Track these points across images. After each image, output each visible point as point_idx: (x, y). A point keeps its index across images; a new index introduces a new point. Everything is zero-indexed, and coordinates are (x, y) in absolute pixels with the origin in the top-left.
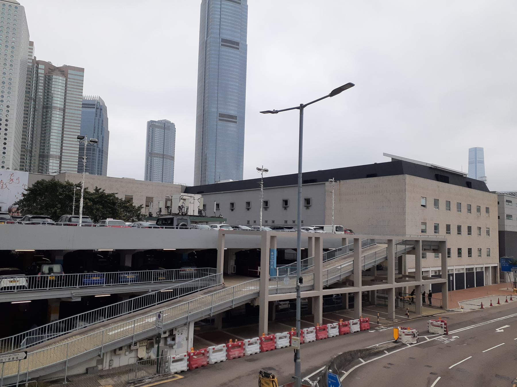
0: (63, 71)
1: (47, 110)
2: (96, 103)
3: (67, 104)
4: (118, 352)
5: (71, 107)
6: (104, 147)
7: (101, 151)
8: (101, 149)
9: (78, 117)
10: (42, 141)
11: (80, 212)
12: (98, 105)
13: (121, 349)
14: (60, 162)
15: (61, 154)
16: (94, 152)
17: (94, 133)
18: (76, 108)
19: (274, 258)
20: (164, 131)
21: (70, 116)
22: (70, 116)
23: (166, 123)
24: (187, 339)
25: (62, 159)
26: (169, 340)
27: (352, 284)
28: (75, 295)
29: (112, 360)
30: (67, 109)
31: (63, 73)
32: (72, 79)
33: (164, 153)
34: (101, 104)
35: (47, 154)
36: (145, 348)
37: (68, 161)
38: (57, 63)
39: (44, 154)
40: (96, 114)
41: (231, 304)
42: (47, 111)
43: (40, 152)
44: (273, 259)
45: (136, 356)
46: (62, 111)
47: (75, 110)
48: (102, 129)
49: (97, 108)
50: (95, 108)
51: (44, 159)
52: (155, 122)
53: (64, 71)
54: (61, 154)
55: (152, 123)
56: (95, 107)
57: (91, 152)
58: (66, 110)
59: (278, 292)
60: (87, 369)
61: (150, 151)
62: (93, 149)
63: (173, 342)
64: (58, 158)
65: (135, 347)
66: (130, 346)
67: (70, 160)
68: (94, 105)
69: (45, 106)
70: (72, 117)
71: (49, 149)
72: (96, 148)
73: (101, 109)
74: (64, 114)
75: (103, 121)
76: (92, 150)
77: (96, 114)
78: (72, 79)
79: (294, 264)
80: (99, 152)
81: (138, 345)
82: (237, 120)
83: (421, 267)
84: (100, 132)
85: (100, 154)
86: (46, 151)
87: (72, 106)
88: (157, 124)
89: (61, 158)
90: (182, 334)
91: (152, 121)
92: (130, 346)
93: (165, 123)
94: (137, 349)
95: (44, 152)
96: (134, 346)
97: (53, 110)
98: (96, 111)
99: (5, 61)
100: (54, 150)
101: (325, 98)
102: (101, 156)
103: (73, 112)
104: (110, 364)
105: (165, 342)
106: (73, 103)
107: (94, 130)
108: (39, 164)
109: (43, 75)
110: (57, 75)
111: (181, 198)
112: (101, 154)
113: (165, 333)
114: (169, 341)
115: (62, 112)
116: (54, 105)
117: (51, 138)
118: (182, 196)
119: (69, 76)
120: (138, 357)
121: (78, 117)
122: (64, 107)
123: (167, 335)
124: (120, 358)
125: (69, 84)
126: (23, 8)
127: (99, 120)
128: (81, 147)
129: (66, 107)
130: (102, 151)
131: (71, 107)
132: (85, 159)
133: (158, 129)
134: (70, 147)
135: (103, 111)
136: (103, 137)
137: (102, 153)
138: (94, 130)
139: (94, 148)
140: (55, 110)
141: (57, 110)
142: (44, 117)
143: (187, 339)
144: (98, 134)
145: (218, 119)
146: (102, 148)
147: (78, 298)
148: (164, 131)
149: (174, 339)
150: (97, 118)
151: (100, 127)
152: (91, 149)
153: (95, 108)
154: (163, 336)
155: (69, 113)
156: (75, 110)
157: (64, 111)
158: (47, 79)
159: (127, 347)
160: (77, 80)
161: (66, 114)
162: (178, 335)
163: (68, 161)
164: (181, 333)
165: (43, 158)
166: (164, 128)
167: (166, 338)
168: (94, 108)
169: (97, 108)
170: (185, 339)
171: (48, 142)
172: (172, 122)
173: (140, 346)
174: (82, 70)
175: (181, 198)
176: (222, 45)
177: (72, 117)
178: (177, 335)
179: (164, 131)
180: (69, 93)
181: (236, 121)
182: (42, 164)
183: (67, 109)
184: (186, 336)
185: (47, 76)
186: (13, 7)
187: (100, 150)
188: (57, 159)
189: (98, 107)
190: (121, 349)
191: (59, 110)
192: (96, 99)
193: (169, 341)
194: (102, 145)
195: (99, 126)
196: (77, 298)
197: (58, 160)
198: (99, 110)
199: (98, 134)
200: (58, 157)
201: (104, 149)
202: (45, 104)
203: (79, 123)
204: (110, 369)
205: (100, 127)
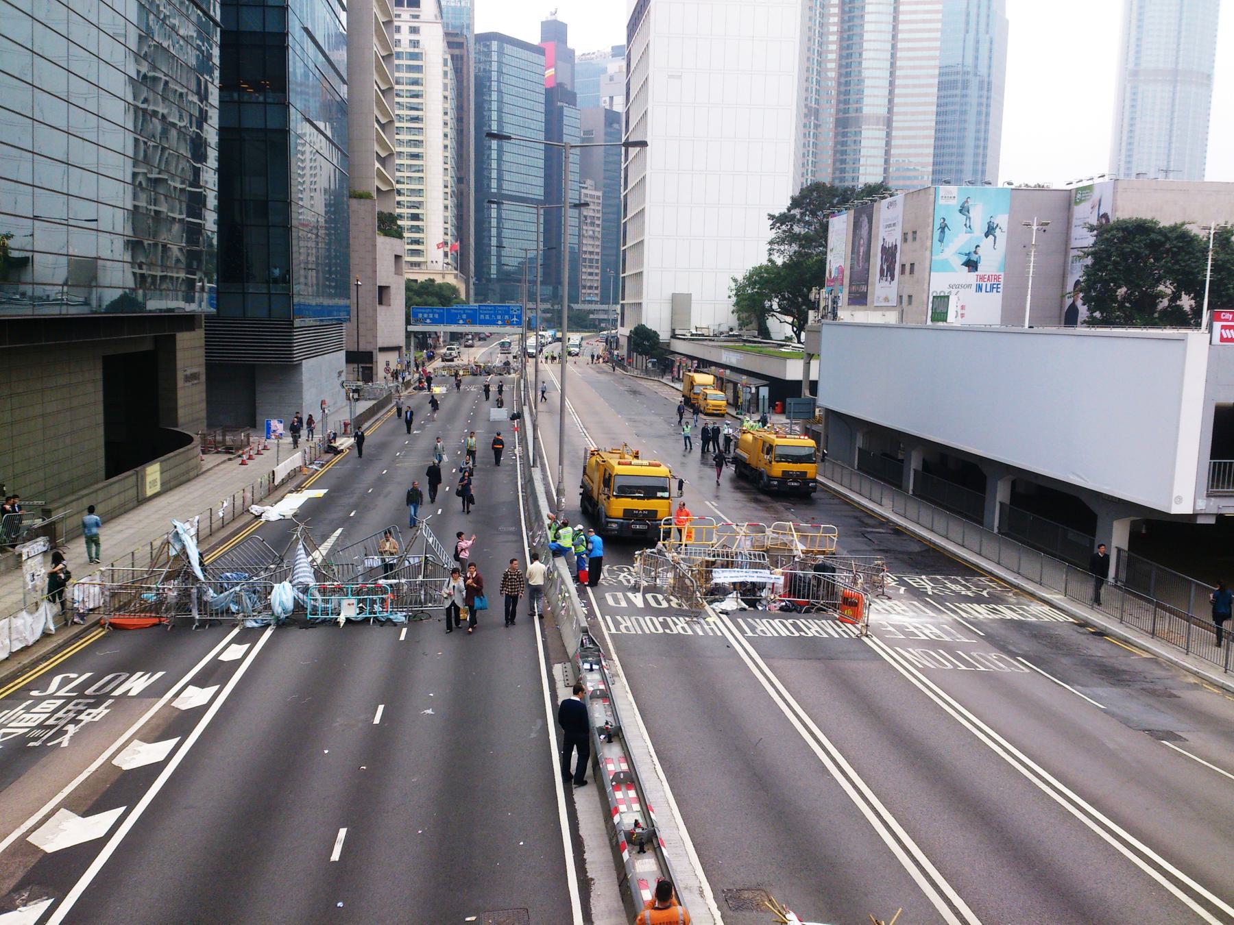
6: (994, 70)
7: (986, 86)
8: (986, 80)
10: (843, 80)
14: (888, 135)
15: (890, 111)
16: (965, 92)
17: (967, 32)
25: (894, 124)
33: (1177, 63)
35: (854, 115)
37: (909, 128)
39: (847, 115)
43: (838, 111)
48: (988, 16)
51: (849, 130)
54: (890, 111)
57: (958, 92)
62: (963, 81)
64: (882, 123)
67: (913, 124)
71: (859, 101)
72: (971, 77)
76: (960, 85)
80: (981, 88)
84: (982, 27)
85: (981, 97)
86: (852, 106)
89: (889, 123)
95: (846, 111)
100: (873, 102)
102: (984, 100)
107: (967, 23)
108: (835, 146)
112: (985, 93)
117: (865, 69)
128: (944, 78)
130: (989, 83)
134: (915, 86)
136: (991, 43)
137: (989, 90)
138: (967, 23)
139: (966, 77)
142: (847, 9)
144: (977, 31)
146: (989, 76)
151: (983, 12)
163: (909, 128)
165: (844, 128)
171: (856, 81)
182: (842, 146)
187: (981, 83)
188: (881, 127)
194: (990, 67)
195: (979, 7)
197: (883, 130)
199: (977, 31)
200: (881, 119)
201: (994, 79)
203: (937, 12)
205: (983, 12)
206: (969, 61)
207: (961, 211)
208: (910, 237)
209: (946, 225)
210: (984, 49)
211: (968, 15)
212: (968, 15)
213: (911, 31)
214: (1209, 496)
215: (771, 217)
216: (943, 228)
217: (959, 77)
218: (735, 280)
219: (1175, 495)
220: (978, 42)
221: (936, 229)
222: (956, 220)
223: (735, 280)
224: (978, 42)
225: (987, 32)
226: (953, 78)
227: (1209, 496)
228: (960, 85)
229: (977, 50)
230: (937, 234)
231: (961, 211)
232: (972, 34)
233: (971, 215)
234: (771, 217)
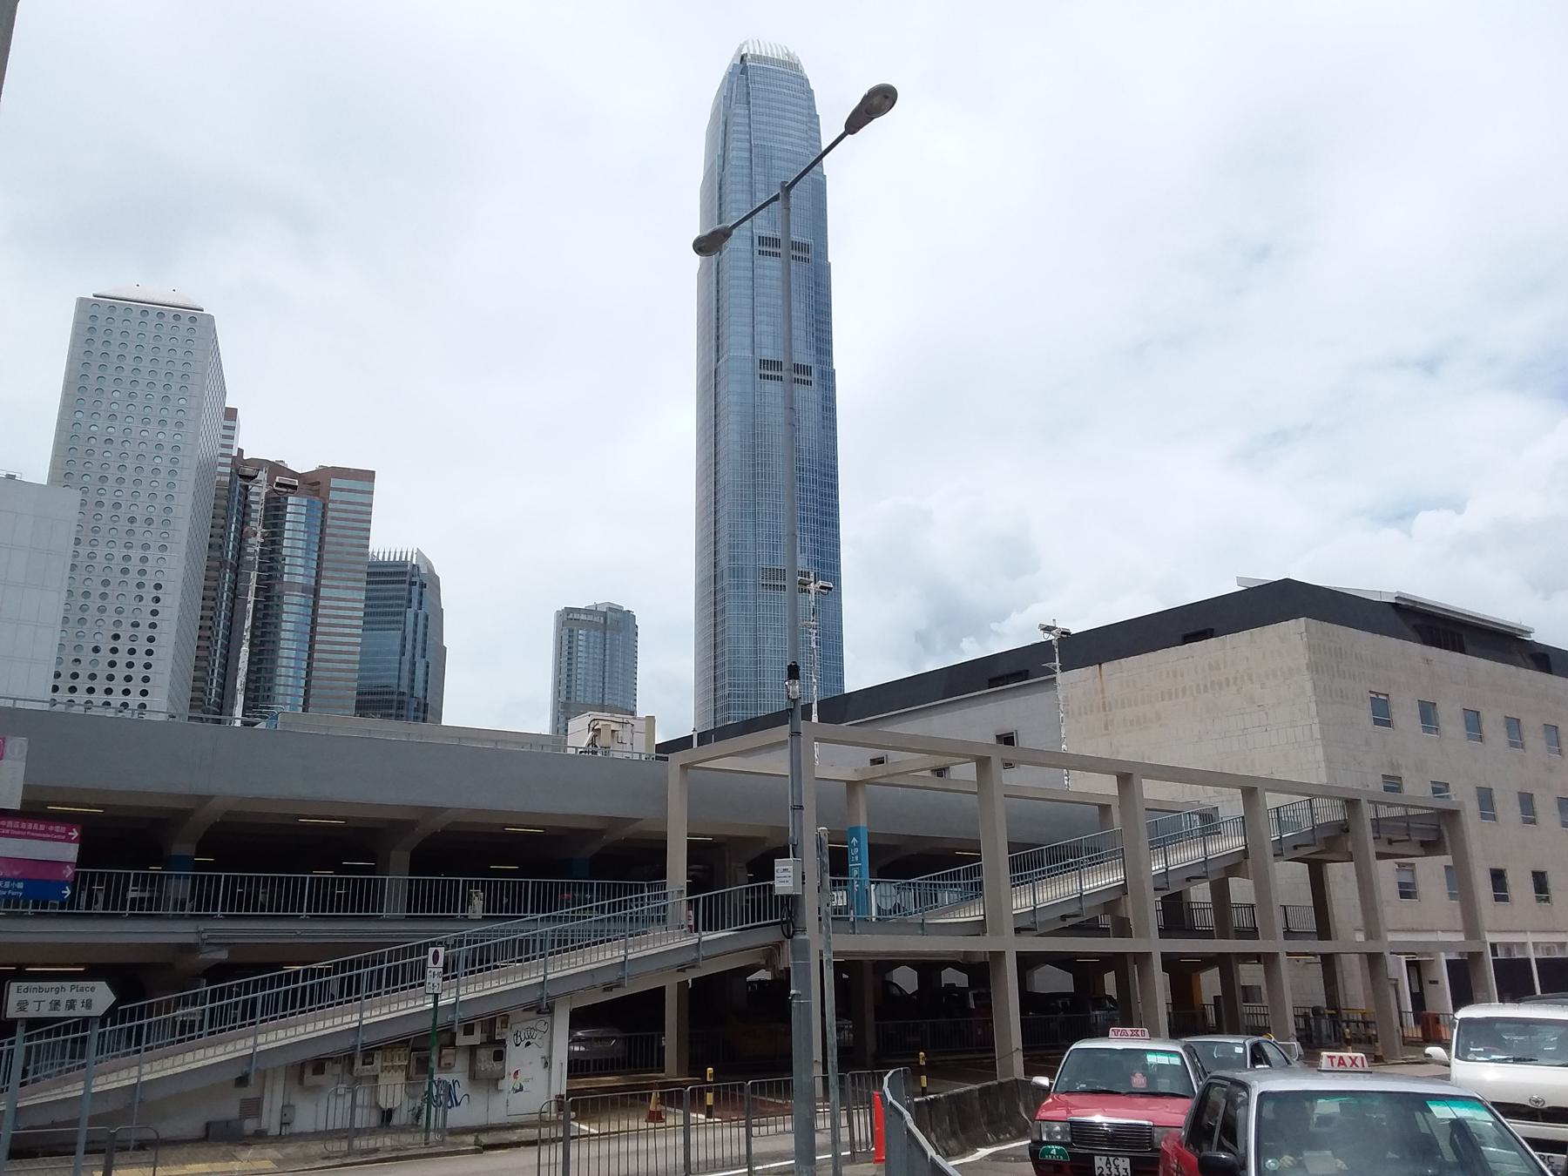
0: (316, 484)
4: (310, 1078)
7: (422, 708)
11: (238, 686)
13: (319, 1066)
19: (859, 854)
21: (332, 608)
24: (546, 1063)
26: (484, 1055)
27: (1122, 928)
28: (209, 937)
29: (292, 1106)
30: (326, 586)
31: (315, 487)
32: (342, 502)
34: (424, 571)
36: (400, 1077)
38: (302, 463)
41: (695, 955)
44: (857, 858)
45: (373, 1104)
52: (578, 610)
53: (319, 483)
55: (568, 615)
56: (407, 578)
58: (323, 592)
59: (856, 931)
60: (208, 1125)
61: (563, 699)
63: (497, 1066)
65: (369, 1067)
66: (350, 1059)
68: (405, 573)
72: (406, 698)
73: (423, 586)
74: (315, 604)
75: (427, 618)
78: (342, 502)
79: (926, 879)
81: (378, 1063)
83: (1382, 928)
90: (528, 1044)
91: (569, 611)
92: (348, 1059)
94: (377, 1076)
96: (364, 1064)
99: (89, 345)
101: (837, 144)
104: (284, 1118)
105: (470, 1060)
111: (592, 726)
113: (469, 1030)
114: (485, 1063)
118: (596, 722)
119: (333, 495)
120: (377, 1104)
123: (476, 1038)
124: (317, 1105)
125: (333, 518)
126: (211, 319)
127: (416, 616)
130: (426, 705)
132: (259, 535)
136: (428, 667)
137: (425, 712)
139: (401, 698)
140: (291, 593)
143: (547, 1064)
146: (426, 698)
147: (219, 950)
149: (499, 1056)
152: (392, 701)
154: (462, 1040)
157: (316, 593)
159: (343, 1071)
160: (358, 504)
162: (517, 1045)
164: (526, 1041)
167: (472, 1050)
168: (404, 582)
169: (413, 584)
170: (539, 1063)
172: (625, 609)
173: (384, 1069)
174: (369, 476)
175: (592, 726)
176: (761, 378)
178: (510, 1046)
184: (546, 1054)
186: (185, 320)
189: (414, 579)
190: (319, 1066)
192: (409, 559)
193: (485, 1063)
196: (215, 948)
198: (416, 589)
204: (283, 1134)
206: (405, 682)
211: (404, 639)
225: (424, 657)
226: (390, 697)
228: (395, 704)
229: (413, 673)
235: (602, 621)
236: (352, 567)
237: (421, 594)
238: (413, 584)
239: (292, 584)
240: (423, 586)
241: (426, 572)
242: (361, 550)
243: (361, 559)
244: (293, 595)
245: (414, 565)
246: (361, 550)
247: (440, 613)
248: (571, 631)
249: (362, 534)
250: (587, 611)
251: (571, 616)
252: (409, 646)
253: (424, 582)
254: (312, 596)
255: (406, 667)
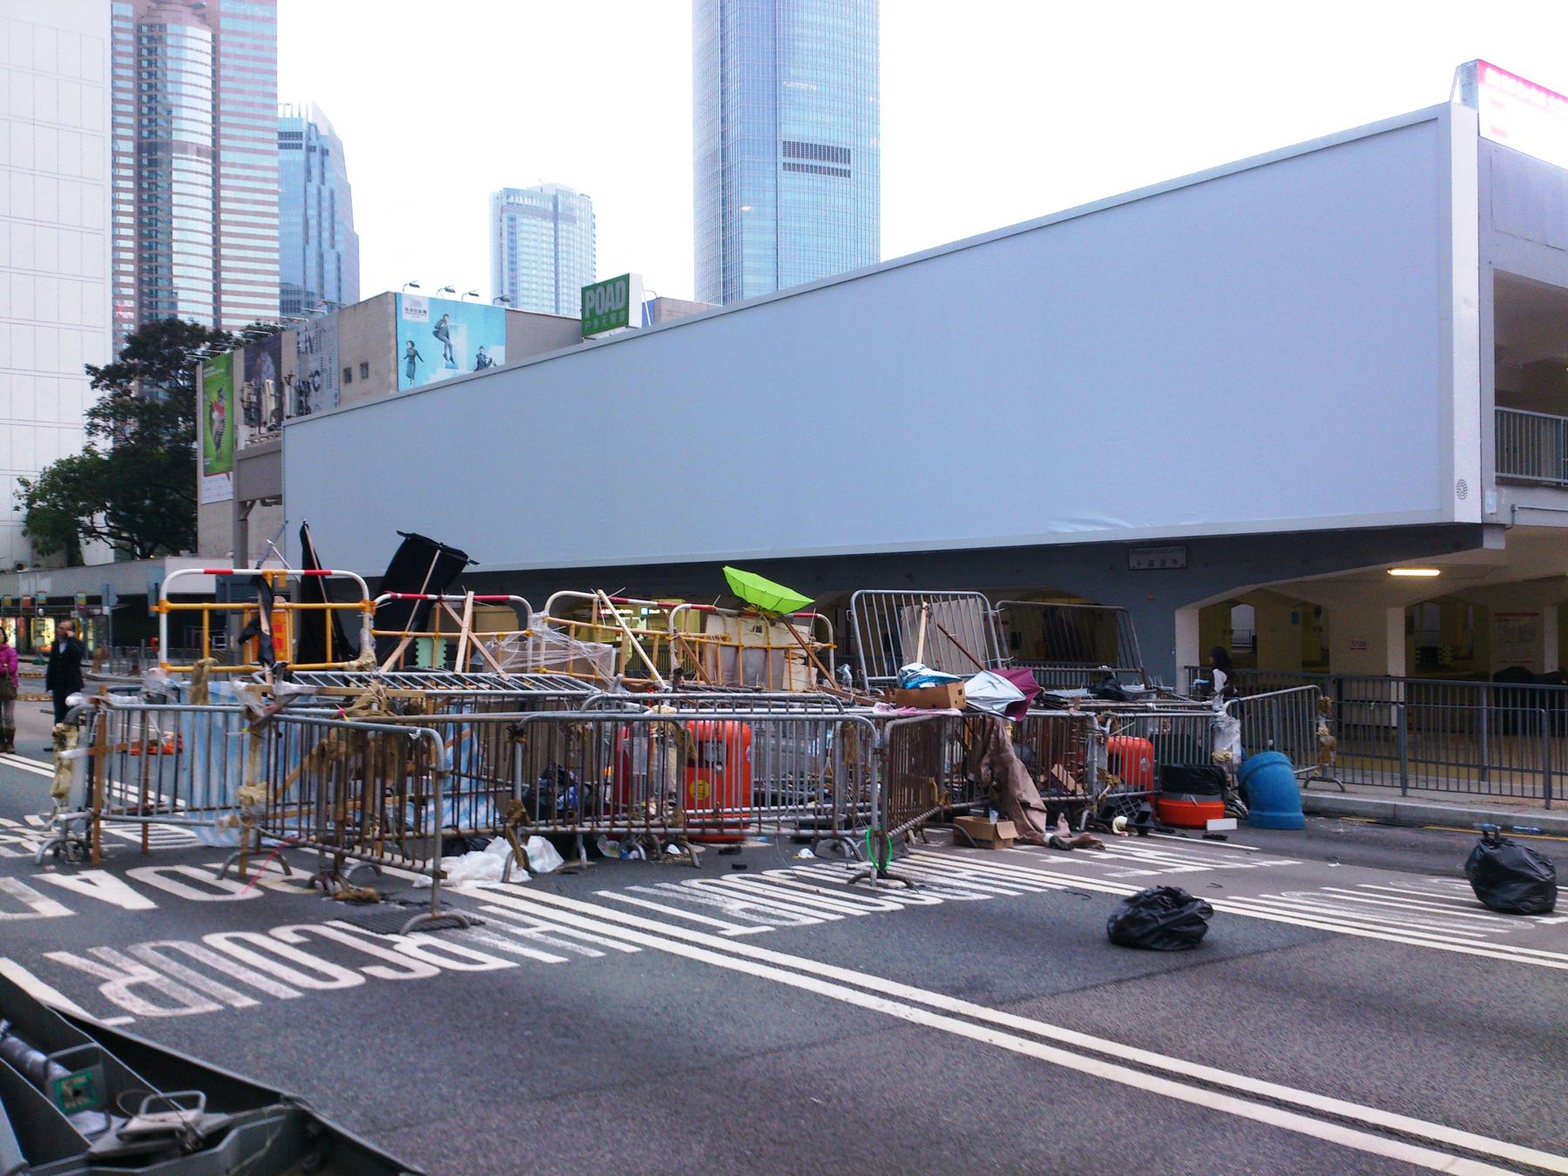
1: (154, 157)
2: (304, 128)
3: (223, 130)
5: (240, 144)
9: (266, 180)
12: (313, 138)
18: (260, 146)
20: (556, 225)
21: (237, 177)
22: (237, 177)
23: (560, 198)
31: (200, 12)
34: (323, 131)
40: (309, 172)
42: (153, 163)
46: (207, 157)
47: (255, 151)
49: (311, 149)
50: (304, 147)
55: (508, 197)
56: (304, 142)
58: (225, 156)
68: (298, 135)
69: (145, 141)
70: (247, 178)
72: (316, 299)
73: (325, 152)
75: (332, 194)
77: (309, 172)
82: (849, 163)
87: (243, 138)
88: (526, 202)
91: (509, 192)
93: (555, 198)
97: (177, 158)
98: (308, 160)
103: (250, 162)
106: (245, 127)
109: (130, 26)
110: (178, 21)
115: (207, 163)
116: (176, 136)
119: (225, 23)
121: (266, 180)
122: (215, 142)
129: (223, 142)
131: (240, 144)
133: (533, 222)
135: (329, 161)
136: (339, 259)
140: (184, 156)
141: (189, 156)
144: (320, 245)
145: (780, 166)
148: (556, 225)
150: (312, 189)
153: (304, 147)
155: (233, 165)
156: (255, 151)
157: (215, 157)
158: (145, 41)
161: (223, 170)
166: (556, 217)
168: (299, 147)
177: (247, 178)
179: (552, 225)
180: (228, 90)
181: (848, 168)
183: (229, 149)
185: (145, 29)
191: (198, 155)
198: (315, 158)
199: (320, 245)
202: (145, 133)
207: (436, 334)
208: (356, 374)
209: (416, 353)
210: (330, 267)
211: (306, 221)
212: (306, 221)
213: (238, 224)
214: (1501, 482)
215: (91, 370)
216: (412, 356)
217: (302, 297)
218: (25, 483)
219: (1457, 479)
220: (321, 256)
221: (400, 359)
222: (431, 348)
223: (25, 483)
224: (321, 256)
227: (1501, 482)
229: (321, 266)
230: (403, 365)
231: (436, 334)
232: (313, 243)
233: (452, 341)
234: (91, 370)
235: (551, 207)
236: (259, 123)
237: (323, 164)
238: (311, 149)
239: (184, 147)
240: (325, 152)
241: (327, 134)
242: (268, 101)
243: (267, 112)
244: (187, 159)
245: (310, 124)
246: (268, 101)
247: (347, 189)
248: (512, 219)
249: (267, 77)
250: (529, 194)
251: (511, 200)
252: (313, 232)
253: (326, 148)
254: (210, 161)
255: (312, 264)
